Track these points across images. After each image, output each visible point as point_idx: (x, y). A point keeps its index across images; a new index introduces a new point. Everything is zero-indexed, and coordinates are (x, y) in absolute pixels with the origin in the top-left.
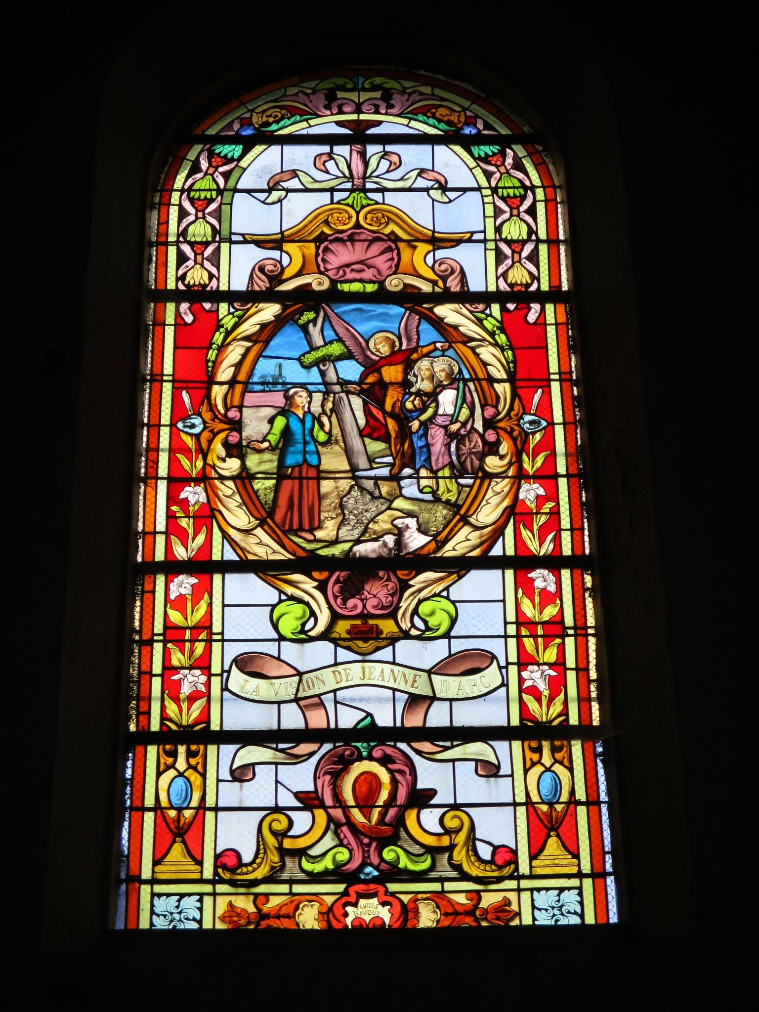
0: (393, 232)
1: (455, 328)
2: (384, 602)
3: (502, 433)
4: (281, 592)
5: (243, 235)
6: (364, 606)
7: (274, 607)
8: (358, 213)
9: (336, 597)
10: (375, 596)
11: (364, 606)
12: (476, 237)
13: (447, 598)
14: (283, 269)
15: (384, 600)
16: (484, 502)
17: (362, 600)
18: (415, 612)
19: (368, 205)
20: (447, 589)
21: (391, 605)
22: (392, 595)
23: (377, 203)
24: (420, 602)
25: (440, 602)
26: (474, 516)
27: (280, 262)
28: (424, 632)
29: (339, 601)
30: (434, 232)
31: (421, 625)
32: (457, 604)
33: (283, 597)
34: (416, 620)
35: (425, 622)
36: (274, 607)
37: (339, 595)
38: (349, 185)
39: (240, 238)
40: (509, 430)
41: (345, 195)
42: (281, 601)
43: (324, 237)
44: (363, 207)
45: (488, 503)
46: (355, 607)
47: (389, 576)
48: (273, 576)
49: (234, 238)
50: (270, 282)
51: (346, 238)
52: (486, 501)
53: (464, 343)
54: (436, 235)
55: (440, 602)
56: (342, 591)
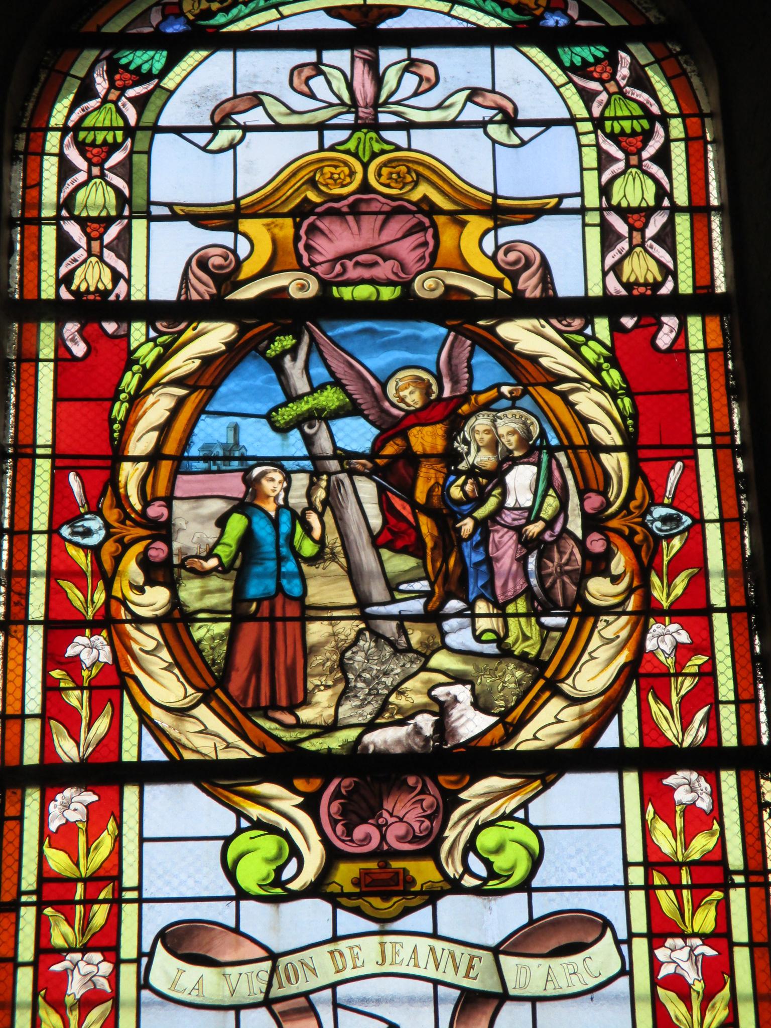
0: (425, 198)
1: (534, 359)
2: (417, 830)
3: (615, 538)
4: (240, 814)
5: (170, 205)
6: (383, 838)
7: (228, 840)
8: (365, 166)
9: (334, 823)
10: (401, 820)
11: (383, 838)
12: (567, 203)
13: (525, 821)
14: (239, 263)
15: (416, 826)
16: (586, 657)
17: (379, 827)
18: (471, 846)
19: (383, 152)
20: (524, 805)
21: (428, 836)
22: (430, 818)
23: (398, 148)
24: (478, 829)
25: (513, 828)
26: (570, 681)
27: (234, 252)
28: (485, 881)
29: (340, 828)
30: (495, 196)
31: (482, 871)
32: (542, 832)
33: (244, 824)
34: (472, 859)
35: (488, 864)
36: (228, 840)
37: (340, 818)
38: (349, 118)
39: (166, 211)
40: (627, 531)
41: (344, 135)
42: (239, 831)
43: (308, 208)
44: (374, 155)
45: (593, 658)
46: (368, 838)
47: (424, 785)
48: (225, 787)
49: (155, 211)
50: (218, 287)
51: (345, 209)
52: (590, 654)
53: (549, 386)
54: (499, 201)
55: (513, 828)
56: (344, 812)
